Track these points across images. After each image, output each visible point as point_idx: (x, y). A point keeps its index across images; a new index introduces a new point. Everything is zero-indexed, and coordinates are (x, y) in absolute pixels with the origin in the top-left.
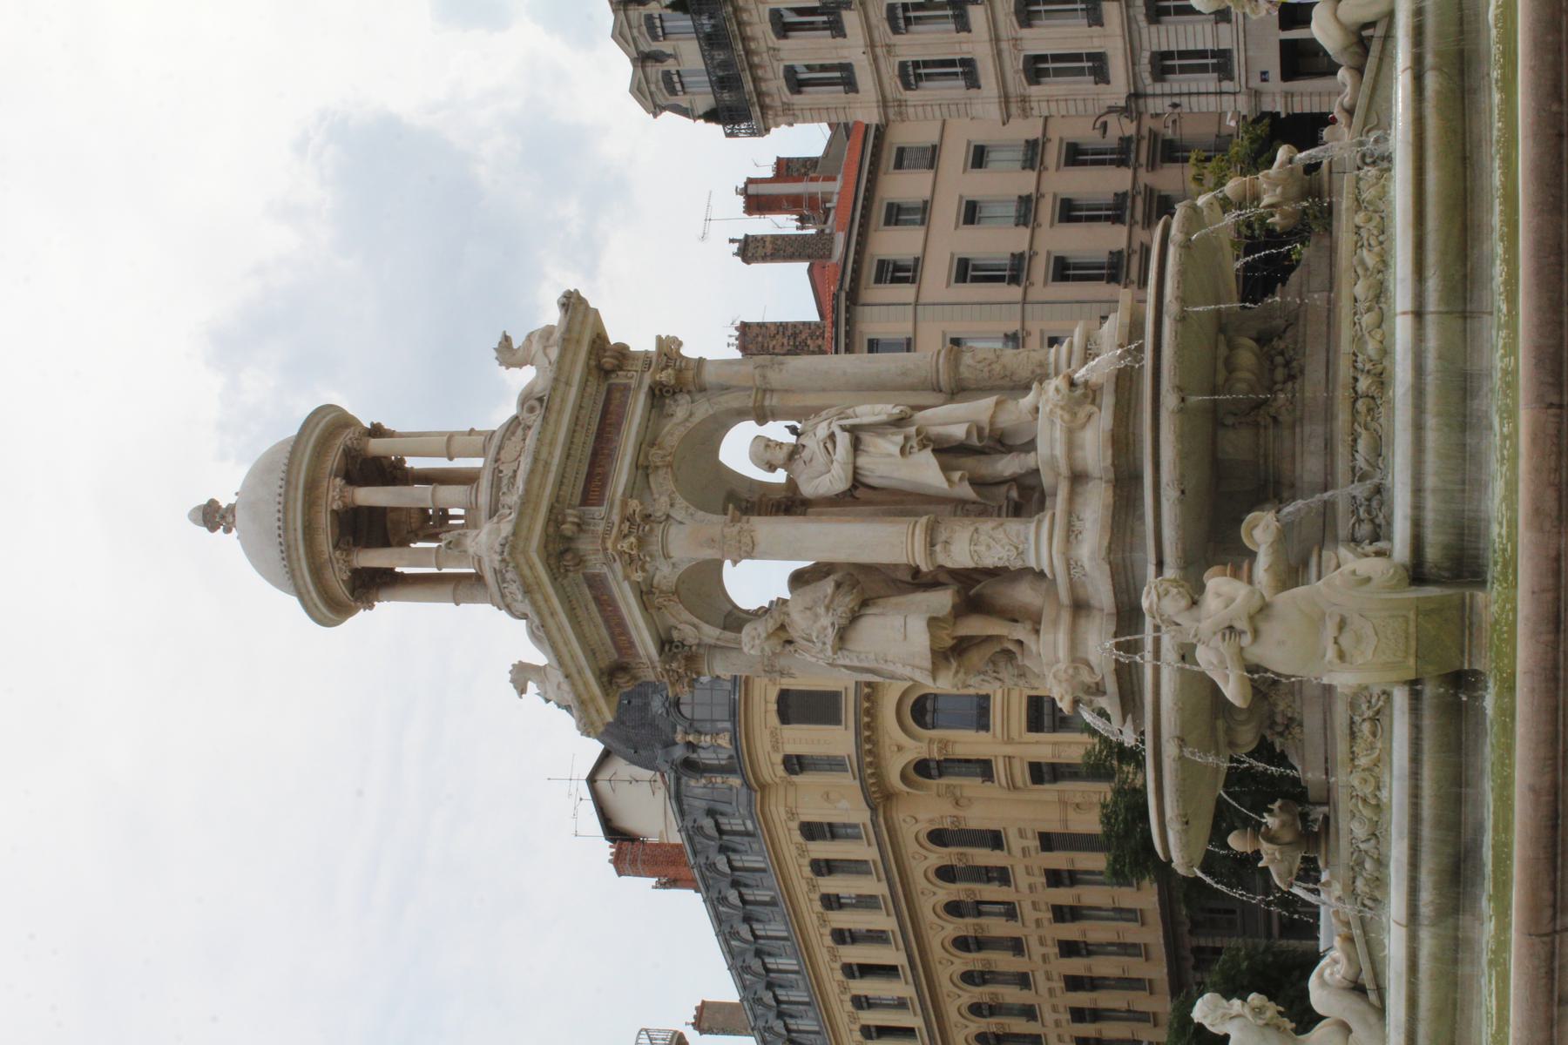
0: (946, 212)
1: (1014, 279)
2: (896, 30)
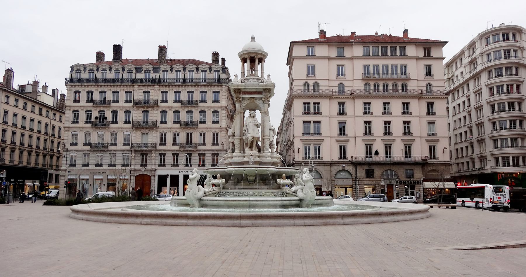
0: (16, 110)
1: (3, 122)
2: (86, 111)
